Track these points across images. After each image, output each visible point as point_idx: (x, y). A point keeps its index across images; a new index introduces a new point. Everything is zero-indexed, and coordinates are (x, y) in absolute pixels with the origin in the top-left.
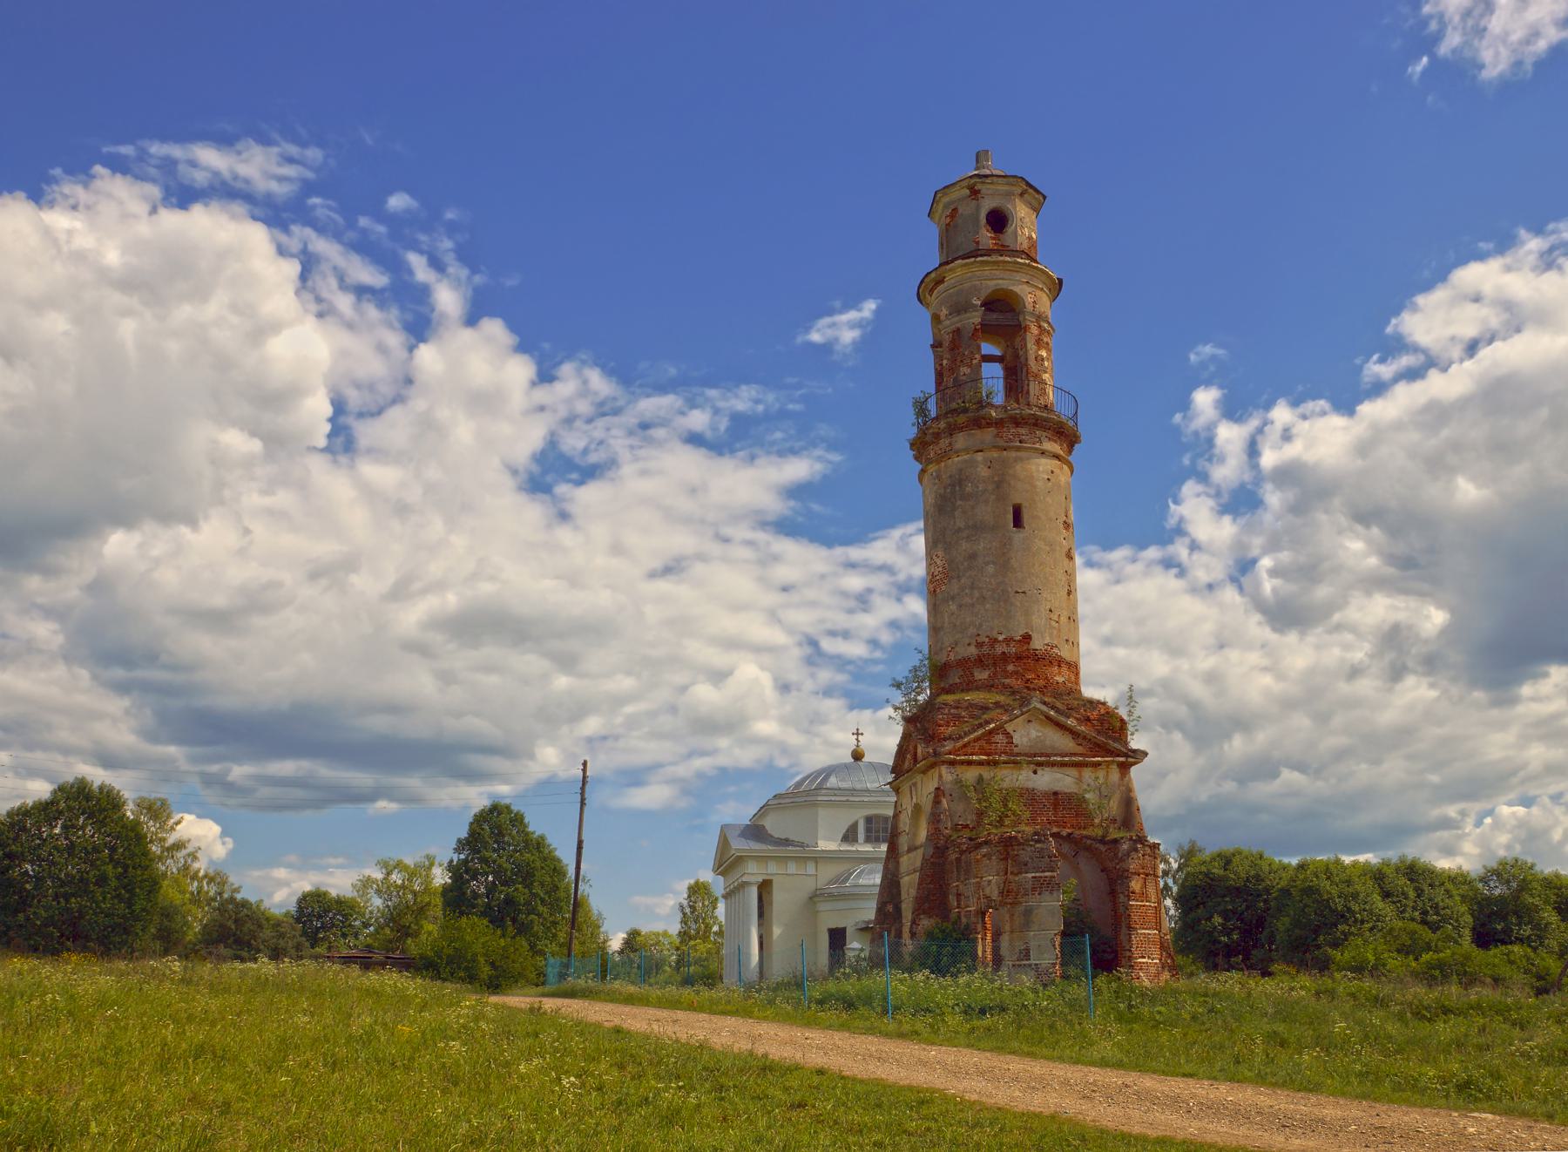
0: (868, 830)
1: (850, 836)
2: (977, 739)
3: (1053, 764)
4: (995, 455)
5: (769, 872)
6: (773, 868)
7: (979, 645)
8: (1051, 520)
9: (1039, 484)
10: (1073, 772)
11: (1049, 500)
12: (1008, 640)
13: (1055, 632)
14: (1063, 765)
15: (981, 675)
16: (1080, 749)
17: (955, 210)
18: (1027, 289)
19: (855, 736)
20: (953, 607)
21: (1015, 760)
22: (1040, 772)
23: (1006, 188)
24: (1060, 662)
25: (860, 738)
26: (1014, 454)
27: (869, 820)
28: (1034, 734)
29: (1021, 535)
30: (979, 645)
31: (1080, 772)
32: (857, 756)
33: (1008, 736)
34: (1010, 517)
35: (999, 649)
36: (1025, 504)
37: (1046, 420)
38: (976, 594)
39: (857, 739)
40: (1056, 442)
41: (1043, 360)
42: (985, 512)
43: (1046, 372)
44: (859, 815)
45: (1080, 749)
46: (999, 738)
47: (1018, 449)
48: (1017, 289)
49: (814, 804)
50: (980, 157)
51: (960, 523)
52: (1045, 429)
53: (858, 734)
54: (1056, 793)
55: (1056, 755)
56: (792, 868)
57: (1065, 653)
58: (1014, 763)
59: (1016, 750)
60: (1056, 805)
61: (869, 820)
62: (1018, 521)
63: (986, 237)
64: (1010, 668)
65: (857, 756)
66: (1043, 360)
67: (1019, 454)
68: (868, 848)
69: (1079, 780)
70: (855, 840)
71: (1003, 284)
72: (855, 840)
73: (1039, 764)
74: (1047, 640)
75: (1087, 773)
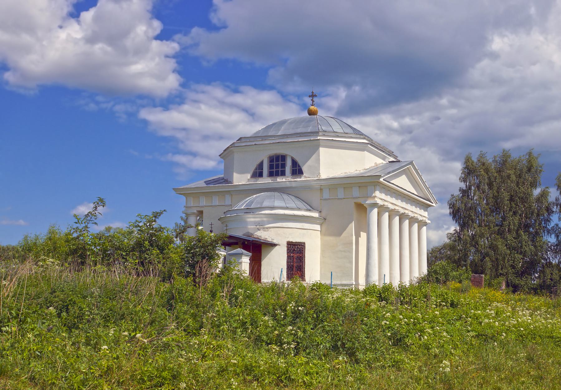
0: (271, 167)
1: (258, 174)
5: (201, 204)
56: (216, 201)
70: (261, 175)
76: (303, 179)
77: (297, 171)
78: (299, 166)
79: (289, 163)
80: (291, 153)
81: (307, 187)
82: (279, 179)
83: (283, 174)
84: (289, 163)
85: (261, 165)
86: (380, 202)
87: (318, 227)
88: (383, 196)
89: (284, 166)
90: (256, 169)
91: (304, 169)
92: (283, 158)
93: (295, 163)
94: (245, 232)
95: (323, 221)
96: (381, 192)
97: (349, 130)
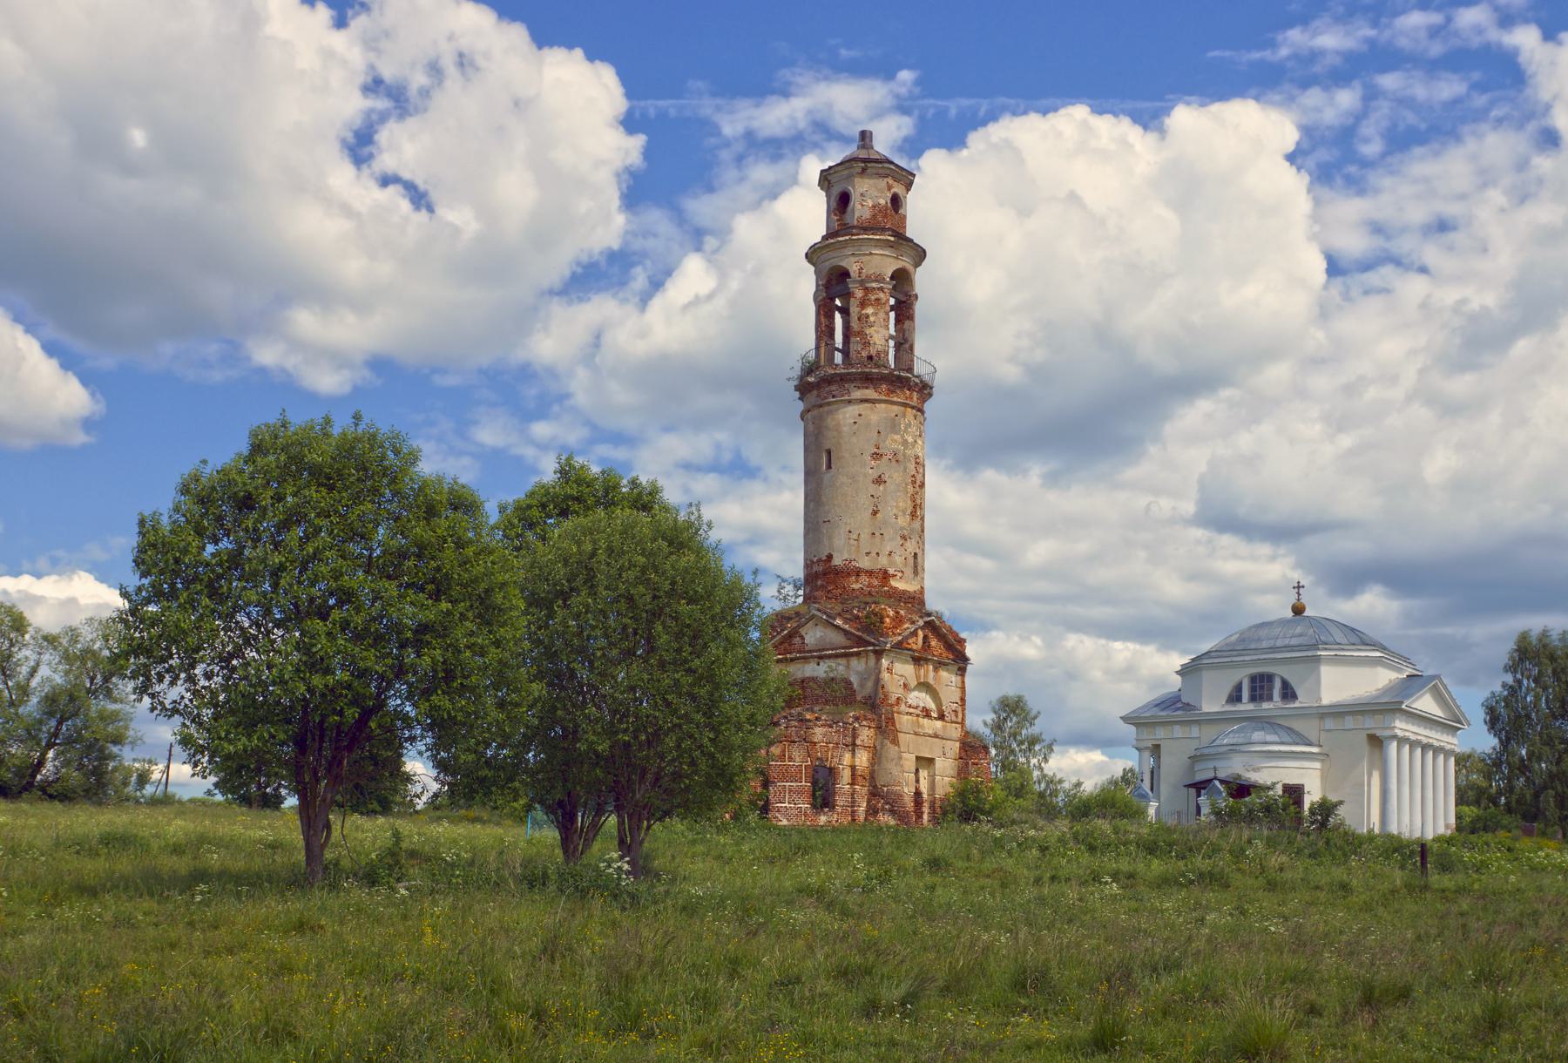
0: (1253, 689)
1: (1235, 697)
2: (782, 643)
3: (830, 657)
6: (1161, 733)
8: (855, 456)
9: (845, 429)
10: (843, 661)
11: (854, 440)
13: (853, 548)
14: (837, 656)
16: (848, 643)
18: (853, 259)
19: (1296, 590)
21: (806, 655)
22: (821, 664)
23: (846, 172)
24: (858, 572)
25: (1301, 590)
26: (826, 409)
27: (1253, 679)
28: (819, 634)
29: (829, 475)
31: (848, 661)
32: (1298, 610)
33: (803, 638)
36: (833, 448)
37: (848, 374)
39: (1299, 594)
40: (867, 388)
41: (868, 317)
43: (870, 327)
44: (1242, 675)
45: (848, 643)
46: (797, 640)
47: (829, 404)
48: (844, 264)
49: (1200, 670)
52: (852, 381)
53: (1299, 587)
55: (828, 650)
56: (1178, 731)
57: (864, 563)
58: (804, 658)
59: (807, 648)
61: (1253, 679)
64: (819, 583)
65: (1298, 610)
66: (868, 317)
67: (830, 408)
68: (1251, 707)
69: (848, 667)
71: (835, 262)
73: (821, 657)
74: (846, 556)
75: (854, 662)
76: (1297, 704)
77: (1289, 693)
78: (1292, 688)
79: (1278, 685)
80: (1279, 671)
81: (1304, 714)
82: (1265, 705)
83: (1270, 698)
84: (1278, 685)
85: (1239, 688)
86: (1400, 733)
87: (1317, 765)
88: (1404, 726)
89: (1271, 689)
90: (1232, 691)
91: (1299, 693)
94: (1230, 772)
95: (1323, 757)
96: (1401, 721)
97: (1354, 639)
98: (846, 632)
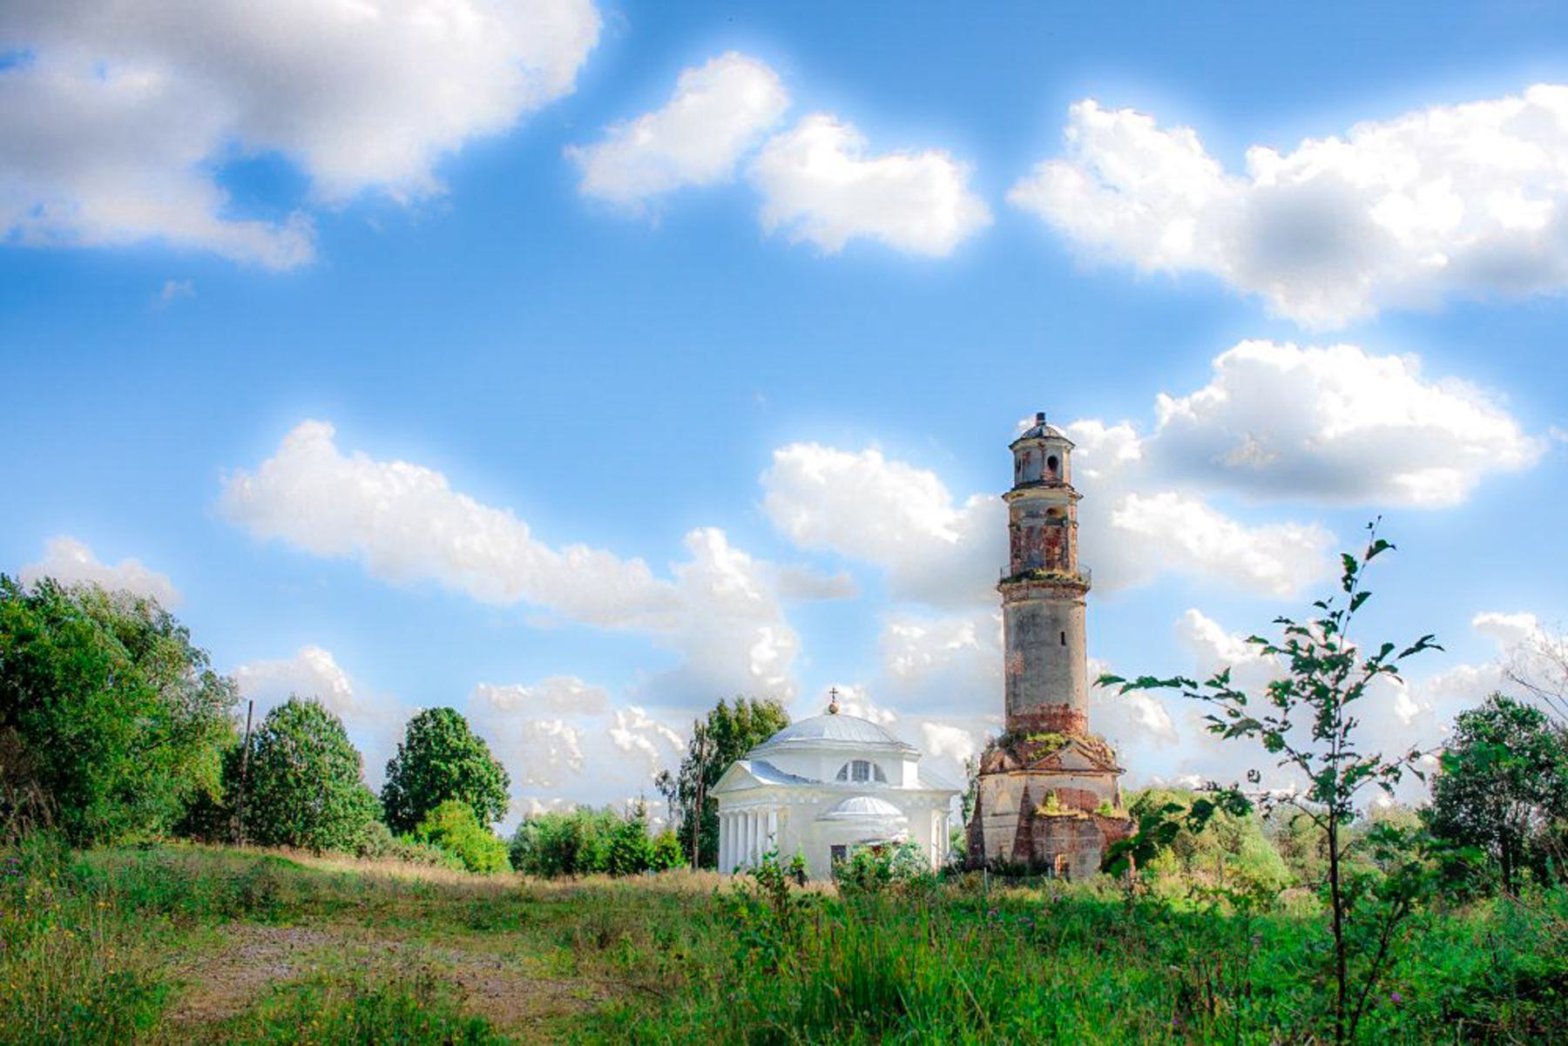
1: (843, 775)
4: (1052, 602)
7: (1043, 708)
12: (1058, 707)
15: (1044, 725)
17: (1029, 453)
20: (1027, 685)
30: (1043, 708)
34: (1060, 639)
35: (1054, 711)
38: (1041, 679)
42: (1045, 635)
44: (848, 760)
50: (1041, 416)
51: (1032, 639)
54: (1081, 791)
60: (1081, 797)
61: (855, 763)
62: (1063, 643)
63: (1048, 474)
72: (845, 778)
85: (845, 770)
89: (867, 771)
92: (867, 764)
93: (877, 769)
98: (1092, 760)
